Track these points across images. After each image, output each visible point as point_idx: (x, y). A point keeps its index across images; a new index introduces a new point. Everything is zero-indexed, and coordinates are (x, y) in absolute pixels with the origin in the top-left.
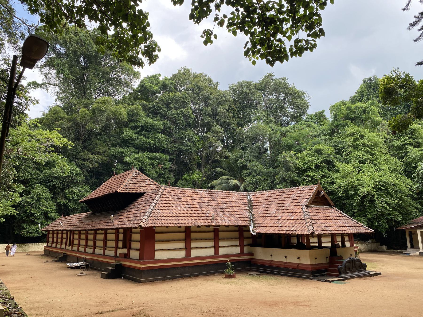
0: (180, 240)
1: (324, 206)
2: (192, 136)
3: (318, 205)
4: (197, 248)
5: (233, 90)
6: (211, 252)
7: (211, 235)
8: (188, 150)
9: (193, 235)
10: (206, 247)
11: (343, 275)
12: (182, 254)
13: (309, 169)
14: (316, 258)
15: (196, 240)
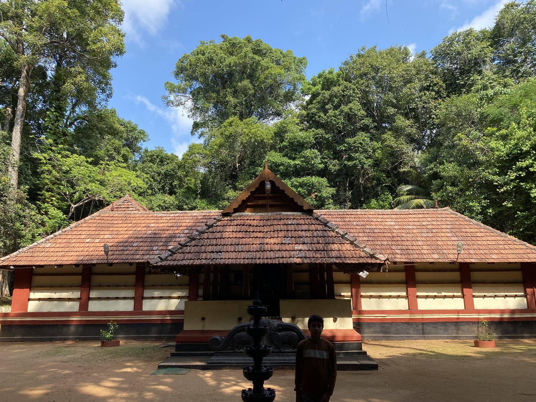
0: (71, 286)
1: (283, 213)
2: (361, 143)
3: (266, 211)
4: (99, 299)
5: (441, 54)
6: (128, 306)
7: (132, 279)
8: (355, 166)
9: (96, 279)
10: (117, 298)
11: (214, 359)
12: (75, 306)
13: (523, 155)
14: (203, 319)
15: (100, 287)
